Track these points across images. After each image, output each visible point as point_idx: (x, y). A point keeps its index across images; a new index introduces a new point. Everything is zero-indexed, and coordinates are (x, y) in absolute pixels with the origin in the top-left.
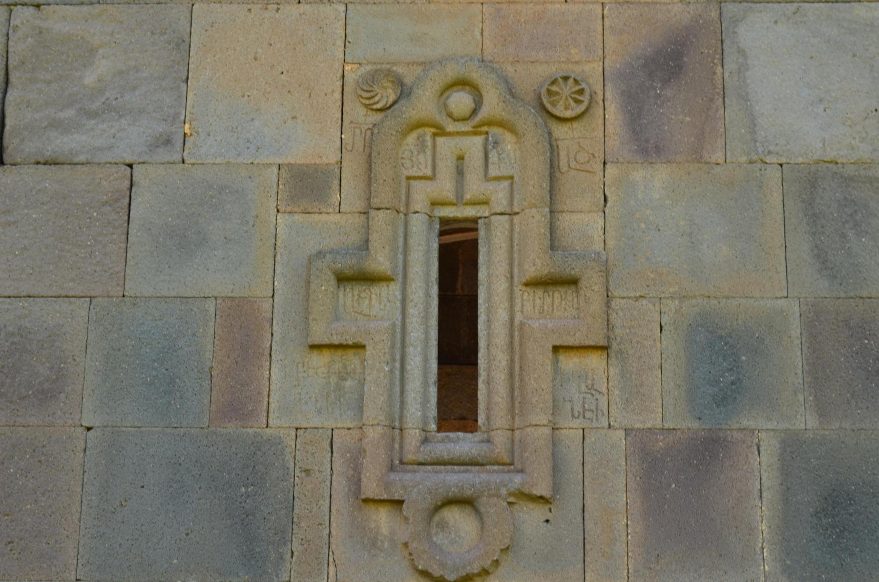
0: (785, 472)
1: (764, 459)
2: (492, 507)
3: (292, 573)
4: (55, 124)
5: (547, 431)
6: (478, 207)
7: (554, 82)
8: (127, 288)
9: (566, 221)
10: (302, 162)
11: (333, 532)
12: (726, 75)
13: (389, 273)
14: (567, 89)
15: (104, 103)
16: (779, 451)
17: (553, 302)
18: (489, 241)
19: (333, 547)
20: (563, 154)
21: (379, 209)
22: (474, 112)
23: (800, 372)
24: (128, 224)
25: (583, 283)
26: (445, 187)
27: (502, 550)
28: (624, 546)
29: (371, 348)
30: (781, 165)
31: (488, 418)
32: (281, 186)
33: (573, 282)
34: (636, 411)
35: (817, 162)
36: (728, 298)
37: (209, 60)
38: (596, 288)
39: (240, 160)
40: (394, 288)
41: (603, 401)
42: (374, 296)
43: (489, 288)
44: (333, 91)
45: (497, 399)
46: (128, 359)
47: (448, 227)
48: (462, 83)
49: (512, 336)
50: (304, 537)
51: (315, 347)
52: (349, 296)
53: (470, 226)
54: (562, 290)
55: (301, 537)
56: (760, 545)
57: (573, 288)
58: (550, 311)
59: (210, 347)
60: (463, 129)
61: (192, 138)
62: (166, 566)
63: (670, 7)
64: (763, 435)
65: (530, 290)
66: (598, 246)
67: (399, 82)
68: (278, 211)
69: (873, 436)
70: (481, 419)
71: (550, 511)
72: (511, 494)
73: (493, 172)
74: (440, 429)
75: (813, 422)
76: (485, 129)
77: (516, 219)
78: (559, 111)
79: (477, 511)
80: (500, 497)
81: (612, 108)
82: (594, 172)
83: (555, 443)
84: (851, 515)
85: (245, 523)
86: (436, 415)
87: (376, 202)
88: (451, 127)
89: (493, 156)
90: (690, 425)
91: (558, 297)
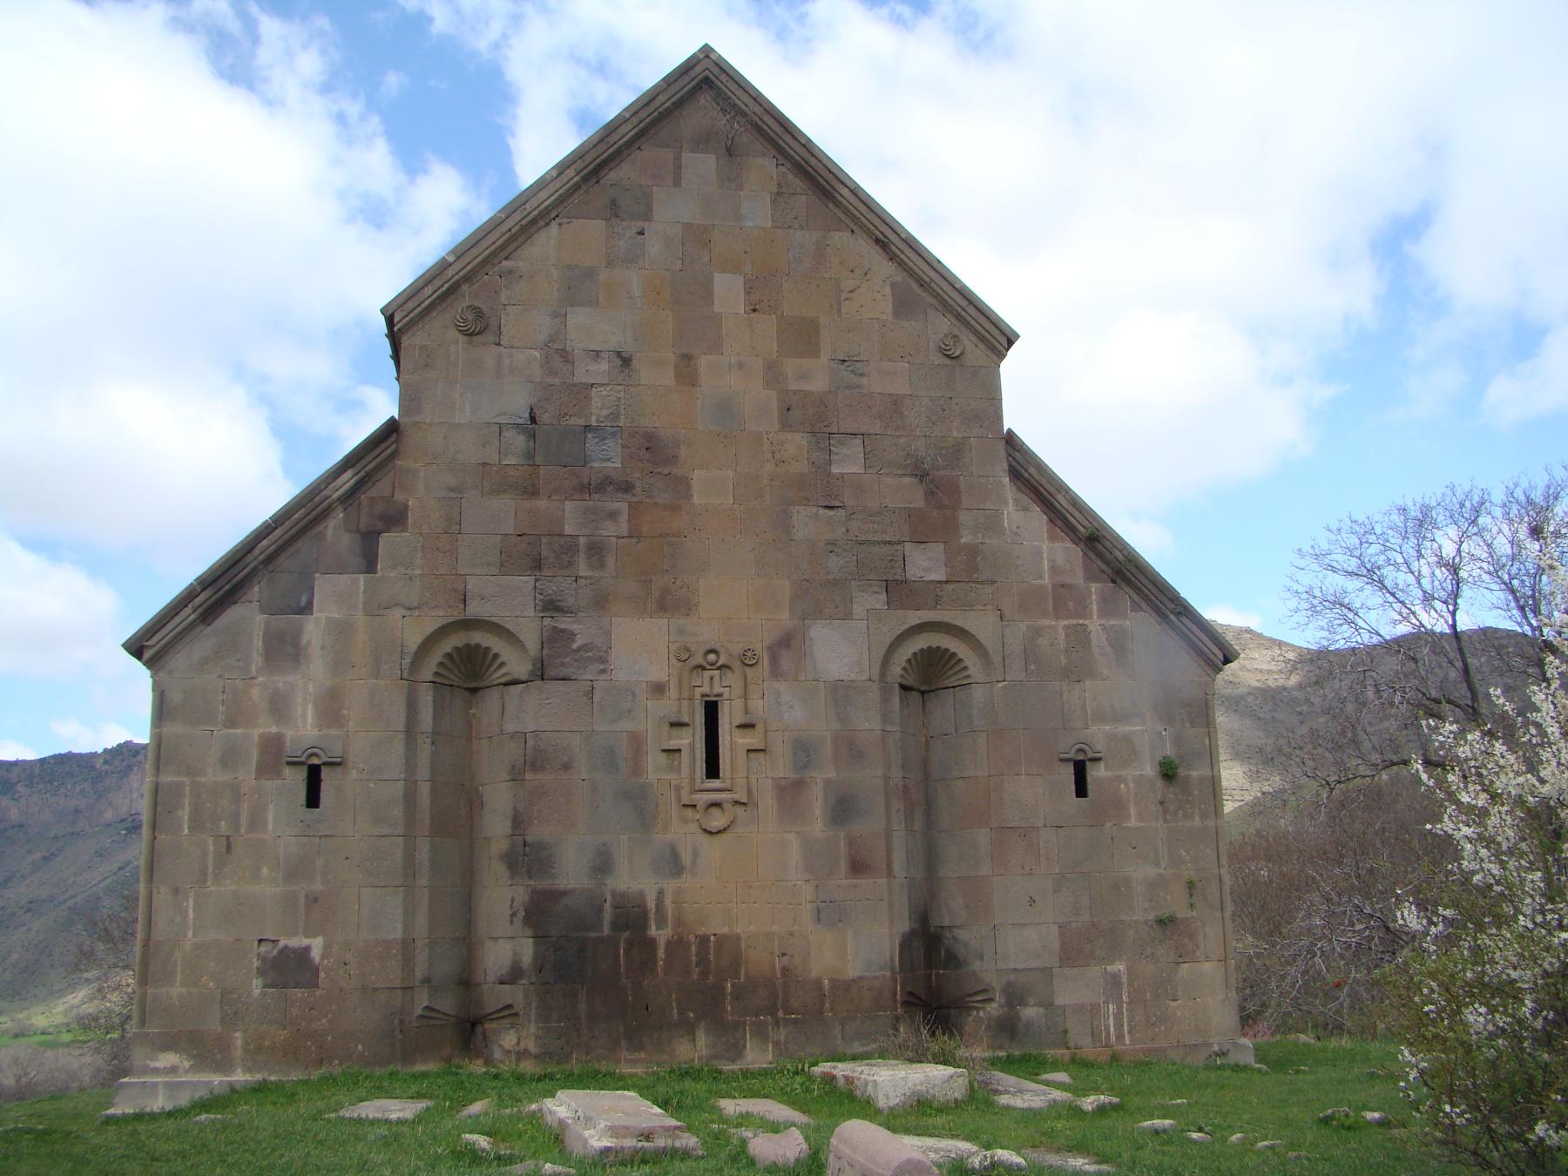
2: (727, 807)
9: (750, 702)
14: (749, 654)
18: (722, 710)
20: (748, 678)
22: (717, 662)
25: (757, 727)
26: (706, 689)
47: (707, 703)
51: (664, 751)
52: (675, 731)
53: (715, 703)
64: (817, 780)
67: (688, 650)
70: (721, 775)
73: (724, 685)
74: (707, 778)
75: (834, 775)
78: (747, 662)
79: (722, 809)
88: (708, 667)
91: (747, 730)
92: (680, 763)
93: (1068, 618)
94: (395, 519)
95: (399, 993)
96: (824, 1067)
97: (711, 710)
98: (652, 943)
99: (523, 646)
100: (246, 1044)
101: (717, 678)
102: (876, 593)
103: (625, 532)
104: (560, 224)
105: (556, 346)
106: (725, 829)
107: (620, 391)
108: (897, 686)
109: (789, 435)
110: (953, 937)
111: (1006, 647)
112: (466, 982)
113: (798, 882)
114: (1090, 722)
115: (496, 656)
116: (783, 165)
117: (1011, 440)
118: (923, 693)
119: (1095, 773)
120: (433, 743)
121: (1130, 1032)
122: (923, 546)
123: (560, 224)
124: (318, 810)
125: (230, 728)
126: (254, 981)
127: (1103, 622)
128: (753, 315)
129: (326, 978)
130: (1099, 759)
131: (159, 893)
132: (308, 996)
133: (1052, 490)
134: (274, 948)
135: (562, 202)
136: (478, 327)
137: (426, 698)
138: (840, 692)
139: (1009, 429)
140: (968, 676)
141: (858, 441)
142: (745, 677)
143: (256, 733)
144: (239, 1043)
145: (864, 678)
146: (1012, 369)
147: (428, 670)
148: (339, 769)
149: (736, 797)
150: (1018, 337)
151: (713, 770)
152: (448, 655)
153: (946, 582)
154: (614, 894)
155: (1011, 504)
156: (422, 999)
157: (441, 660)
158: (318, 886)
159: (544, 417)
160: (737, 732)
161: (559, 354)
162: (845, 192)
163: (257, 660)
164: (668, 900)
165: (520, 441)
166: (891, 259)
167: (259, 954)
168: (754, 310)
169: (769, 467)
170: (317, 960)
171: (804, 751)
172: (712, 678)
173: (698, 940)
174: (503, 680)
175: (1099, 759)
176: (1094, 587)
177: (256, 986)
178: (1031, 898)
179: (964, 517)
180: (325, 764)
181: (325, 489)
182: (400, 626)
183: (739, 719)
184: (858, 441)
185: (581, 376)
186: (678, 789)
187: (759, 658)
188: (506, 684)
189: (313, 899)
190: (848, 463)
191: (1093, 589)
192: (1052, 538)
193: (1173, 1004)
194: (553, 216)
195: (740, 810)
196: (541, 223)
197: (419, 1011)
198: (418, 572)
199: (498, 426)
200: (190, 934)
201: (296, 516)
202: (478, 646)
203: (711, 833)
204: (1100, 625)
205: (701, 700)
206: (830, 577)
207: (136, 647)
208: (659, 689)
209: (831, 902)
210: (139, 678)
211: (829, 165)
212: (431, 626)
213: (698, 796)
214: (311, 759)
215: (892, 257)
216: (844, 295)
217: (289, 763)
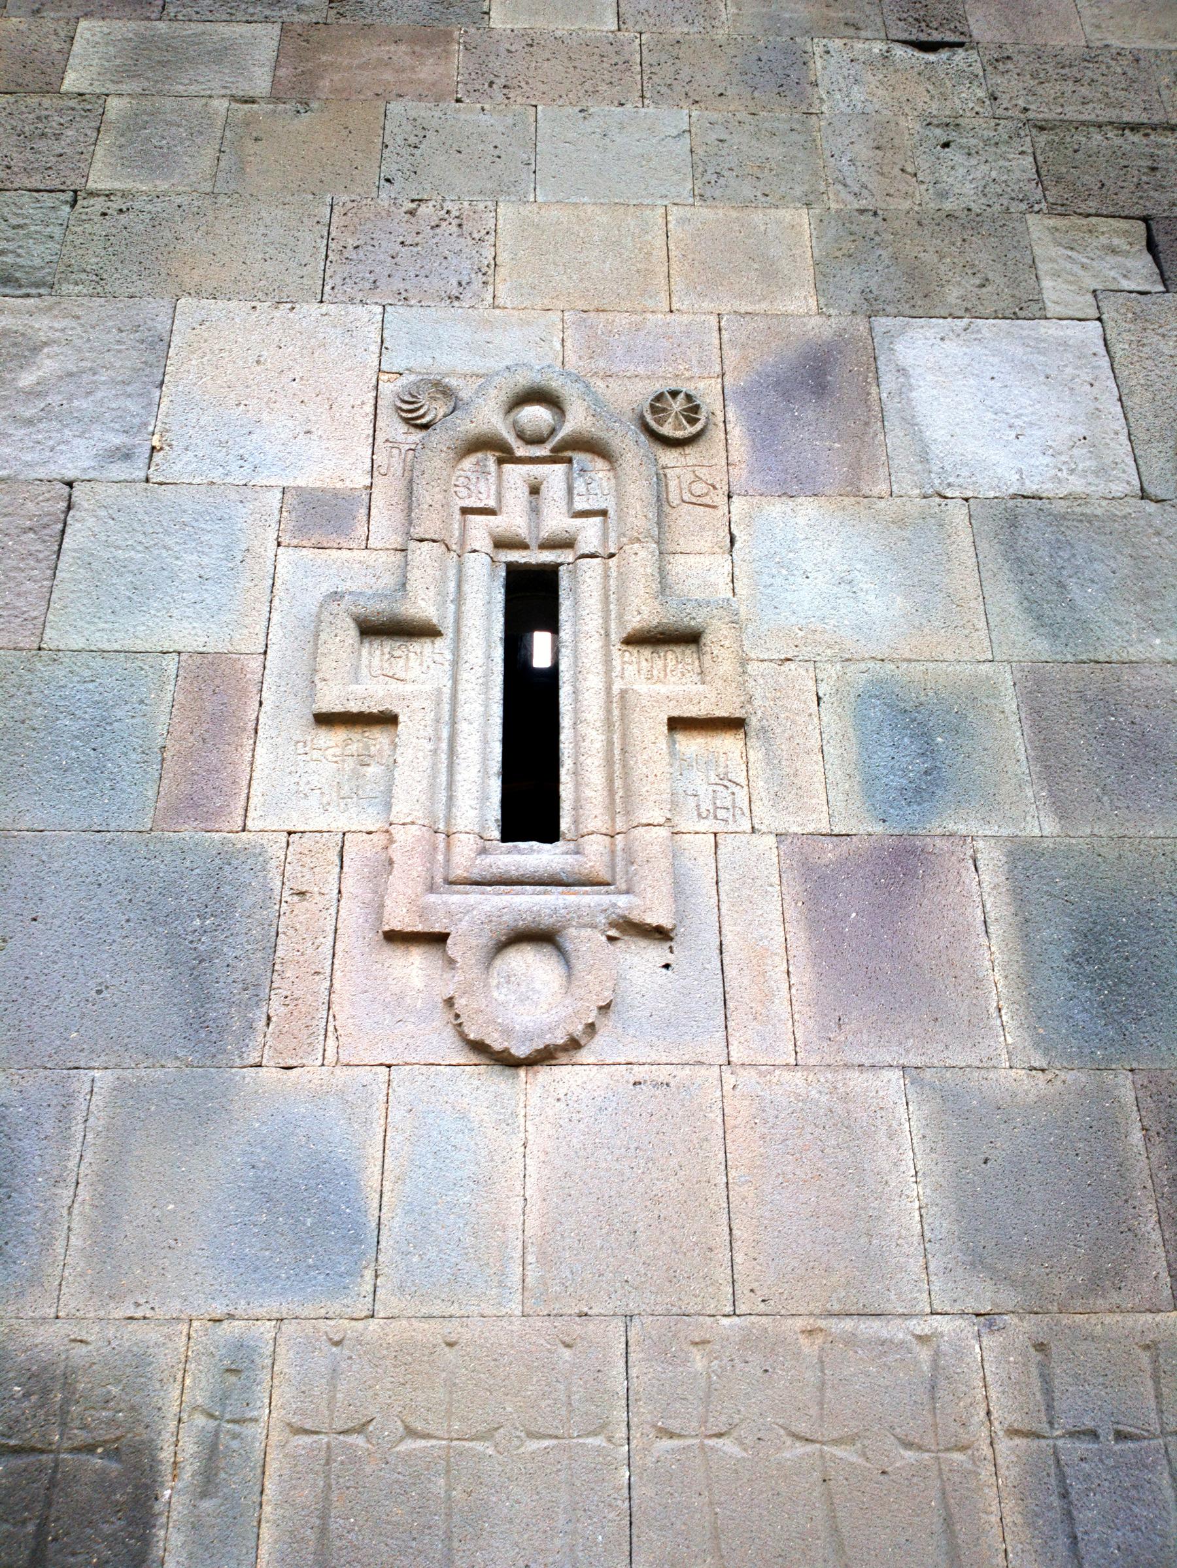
0: (1019, 896)
1: (986, 878)
3: (266, 1051)
5: (664, 832)
6: (559, 552)
8: (46, 638)
9: (678, 566)
10: (318, 484)
11: (336, 986)
12: (884, 395)
13: (435, 621)
15: (43, 410)
16: (1006, 866)
17: (665, 666)
18: (573, 590)
19: (335, 1008)
20: (673, 484)
21: (421, 540)
22: (553, 431)
23: (1023, 758)
24: (58, 557)
25: (707, 639)
26: (514, 520)
27: (600, 1008)
28: (787, 1003)
29: (406, 719)
30: (967, 500)
31: (576, 822)
32: (285, 514)
33: (690, 638)
34: (790, 809)
35: (1014, 497)
36: (909, 661)
37: (193, 362)
38: (727, 643)
39: (229, 480)
41: (742, 794)
42: (412, 655)
44: (363, 403)
45: (588, 793)
46: (34, 734)
49: (609, 711)
50: (289, 993)
51: (325, 720)
52: (377, 653)
54: (679, 650)
55: (285, 993)
56: (995, 1005)
57: (693, 647)
58: (662, 676)
59: (164, 718)
60: (538, 454)
61: (161, 453)
62: (58, 1043)
63: (805, 320)
64: (980, 844)
65: (634, 650)
68: (279, 545)
69: (1142, 847)
70: (565, 824)
71: (672, 952)
72: (613, 925)
73: (580, 505)
74: (505, 838)
76: (568, 454)
77: (612, 562)
78: (667, 430)
80: (596, 927)
81: (736, 432)
82: (714, 507)
84: (1127, 959)
85: (196, 973)
86: (499, 817)
87: (418, 532)
88: (521, 451)
89: (579, 486)
90: (870, 830)
91: (673, 658)
102: (1114, 251)
106: (574, 1044)
142: (661, 479)
145: (1118, 489)
172: (535, 490)
203: (507, 1061)
206: (948, 206)
209: (1120, 1436)
213: (455, 899)
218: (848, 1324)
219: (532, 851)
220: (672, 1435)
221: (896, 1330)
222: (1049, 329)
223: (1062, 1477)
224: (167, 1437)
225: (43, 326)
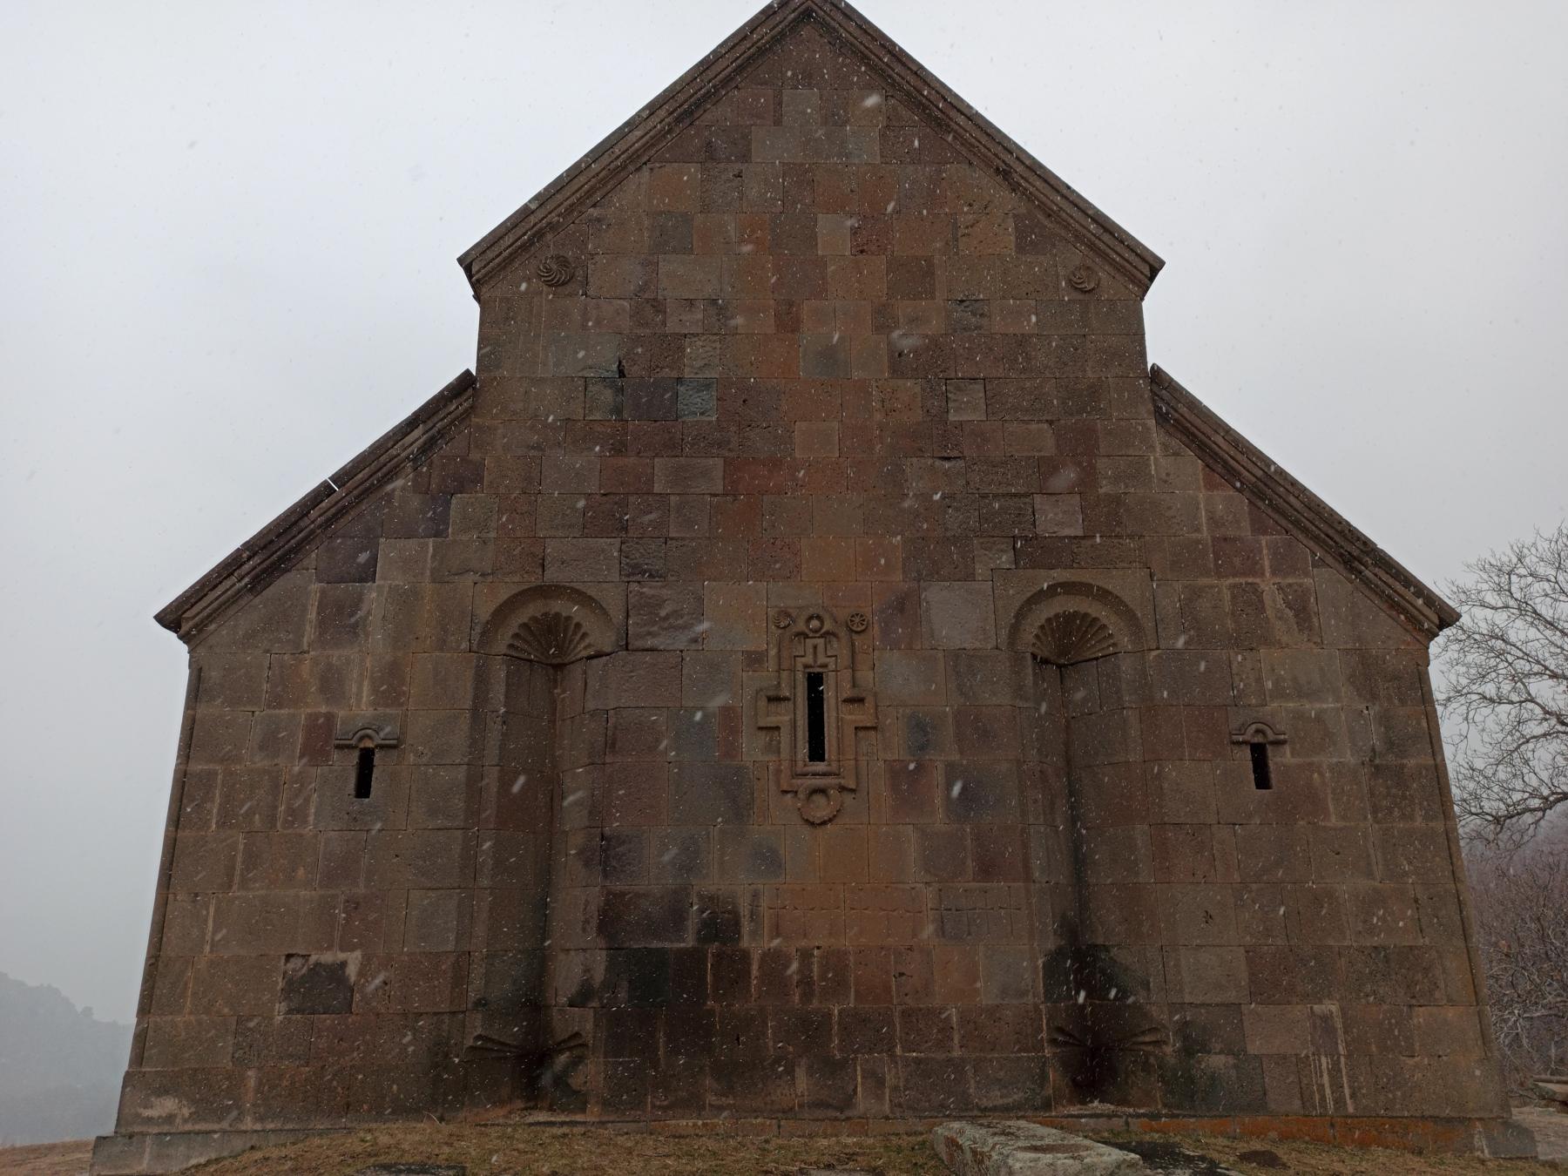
4: (649, 633)
7: (853, 616)
9: (858, 674)
14: (857, 620)
22: (821, 628)
25: (866, 701)
26: (809, 659)
33: (861, 700)
35: (959, 649)
40: (791, 702)
43: (828, 702)
48: (819, 617)
51: (761, 728)
52: (773, 706)
66: (872, 685)
67: (789, 615)
73: (829, 654)
75: (958, 757)
77: (839, 673)
78: (854, 628)
83: (857, 767)
89: (828, 647)
92: (779, 742)
93: (1234, 575)
94: (467, 479)
95: (446, 1019)
96: (950, 1129)
97: (815, 681)
98: (745, 956)
99: (605, 613)
100: (260, 1084)
101: (821, 649)
103: (720, 490)
104: (651, 169)
105: (646, 296)
106: (830, 820)
107: (714, 341)
108: (1029, 656)
109: (900, 382)
110: (1111, 958)
111: (1157, 610)
112: (534, 1005)
113: (917, 885)
114: (1268, 699)
115: (578, 625)
116: (892, 96)
117: (1158, 377)
118: (1060, 666)
119: (1280, 760)
120: (504, 722)
121: (1353, 1096)
122: (1054, 498)
123: (651, 169)
124: (367, 800)
125: (274, 708)
126: (277, 1005)
127: (1278, 580)
128: (861, 257)
129: (361, 1001)
130: (1283, 742)
131: (175, 900)
132: (339, 1024)
133: (1209, 431)
134: (303, 965)
135: (653, 145)
136: (562, 277)
137: (499, 672)
138: (962, 662)
139: (1154, 364)
140: (1114, 645)
141: (979, 386)
142: (853, 645)
143: (303, 714)
144: (252, 1083)
146: (1155, 305)
147: (501, 644)
148: (395, 753)
149: (843, 782)
150: (1162, 263)
151: (817, 753)
152: (525, 626)
153: (1084, 538)
154: (701, 897)
155: (1158, 450)
156: (477, 1026)
157: (517, 631)
158: (361, 890)
159: (634, 371)
160: (844, 708)
161: (650, 304)
162: (961, 120)
163: (309, 634)
164: (764, 903)
165: (608, 395)
166: (1014, 190)
167: (285, 973)
168: (862, 252)
169: (878, 416)
170: (353, 979)
171: (922, 731)
172: (815, 647)
173: (799, 954)
174: (584, 654)
175: (1283, 742)
176: (1264, 540)
177: (280, 1008)
178: (1207, 912)
179: (1101, 464)
180: (382, 747)
181: (392, 447)
182: (471, 594)
183: (847, 694)
184: (979, 386)
185: (672, 326)
186: (778, 772)
187: (868, 621)
188: (590, 658)
189: (354, 905)
190: (967, 409)
191: (1264, 543)
192: (1210, 486)
193: (1411, 1062)
194: (645, 159)
195: (848, 798)
196: (631, 168)
197: (469, 1042)
198: (493, 535)
199: (583, 380)
200: (207, 948)
201: (360, 476)
202: (557, 615)
203: (812, 824)
204: (1274, 584)
205: (804, 672)
207: (171, 619)
208: (754, 660)
209: (957, 910)
210: (175, 653)
211: (943, 91)
212: (504, 594)
214: (364, 741)
215: (1015, 188)
216: (962, 231)
217: (338, 747)
218: (895, 885)
219: (817, 765)
220: (854, 909)
221: (907, 887)
222: (975, 585)
223: (942, 919)
224: (741, 910)
225: (665, 592)
